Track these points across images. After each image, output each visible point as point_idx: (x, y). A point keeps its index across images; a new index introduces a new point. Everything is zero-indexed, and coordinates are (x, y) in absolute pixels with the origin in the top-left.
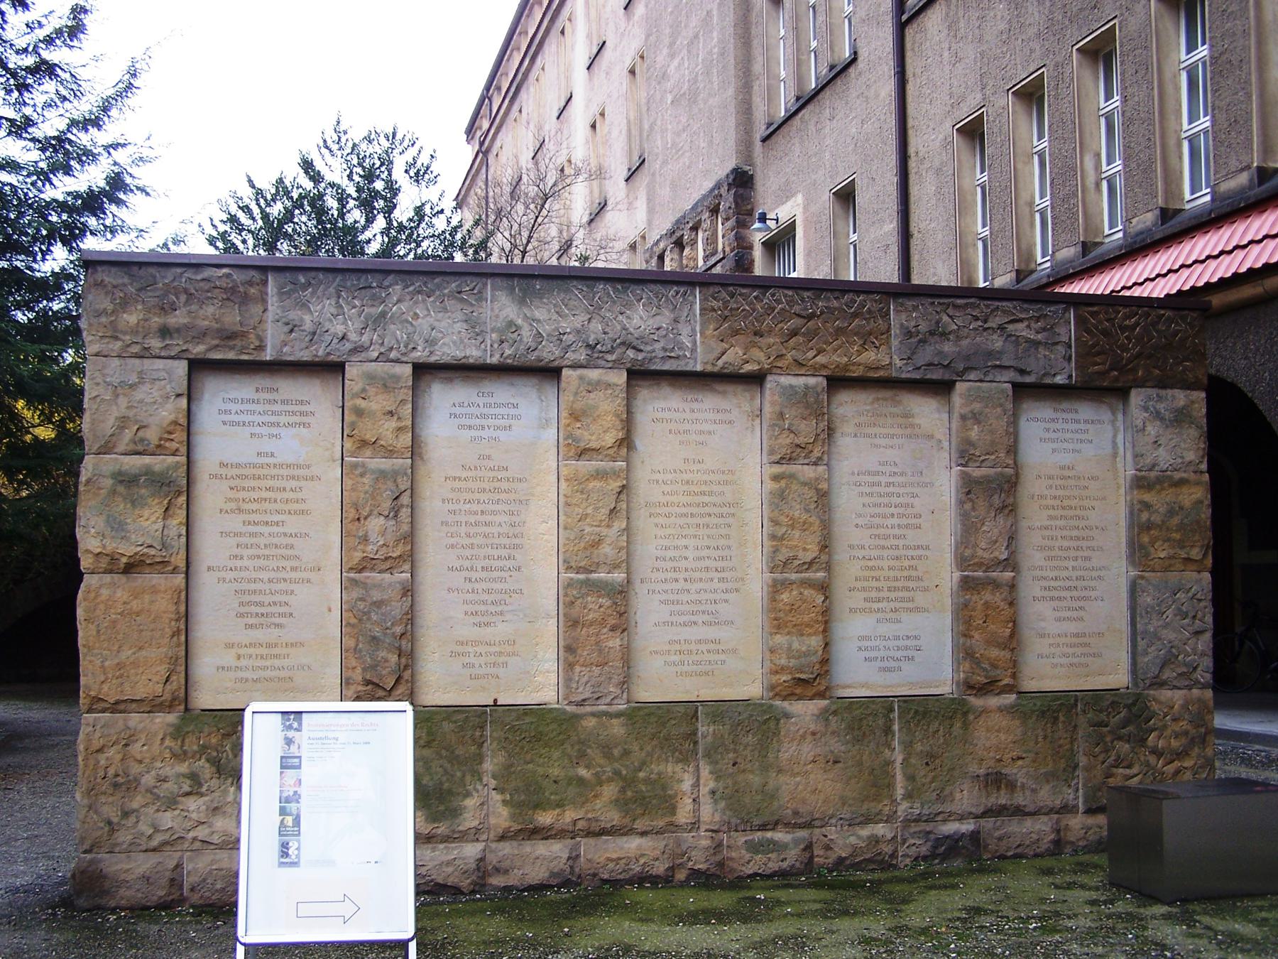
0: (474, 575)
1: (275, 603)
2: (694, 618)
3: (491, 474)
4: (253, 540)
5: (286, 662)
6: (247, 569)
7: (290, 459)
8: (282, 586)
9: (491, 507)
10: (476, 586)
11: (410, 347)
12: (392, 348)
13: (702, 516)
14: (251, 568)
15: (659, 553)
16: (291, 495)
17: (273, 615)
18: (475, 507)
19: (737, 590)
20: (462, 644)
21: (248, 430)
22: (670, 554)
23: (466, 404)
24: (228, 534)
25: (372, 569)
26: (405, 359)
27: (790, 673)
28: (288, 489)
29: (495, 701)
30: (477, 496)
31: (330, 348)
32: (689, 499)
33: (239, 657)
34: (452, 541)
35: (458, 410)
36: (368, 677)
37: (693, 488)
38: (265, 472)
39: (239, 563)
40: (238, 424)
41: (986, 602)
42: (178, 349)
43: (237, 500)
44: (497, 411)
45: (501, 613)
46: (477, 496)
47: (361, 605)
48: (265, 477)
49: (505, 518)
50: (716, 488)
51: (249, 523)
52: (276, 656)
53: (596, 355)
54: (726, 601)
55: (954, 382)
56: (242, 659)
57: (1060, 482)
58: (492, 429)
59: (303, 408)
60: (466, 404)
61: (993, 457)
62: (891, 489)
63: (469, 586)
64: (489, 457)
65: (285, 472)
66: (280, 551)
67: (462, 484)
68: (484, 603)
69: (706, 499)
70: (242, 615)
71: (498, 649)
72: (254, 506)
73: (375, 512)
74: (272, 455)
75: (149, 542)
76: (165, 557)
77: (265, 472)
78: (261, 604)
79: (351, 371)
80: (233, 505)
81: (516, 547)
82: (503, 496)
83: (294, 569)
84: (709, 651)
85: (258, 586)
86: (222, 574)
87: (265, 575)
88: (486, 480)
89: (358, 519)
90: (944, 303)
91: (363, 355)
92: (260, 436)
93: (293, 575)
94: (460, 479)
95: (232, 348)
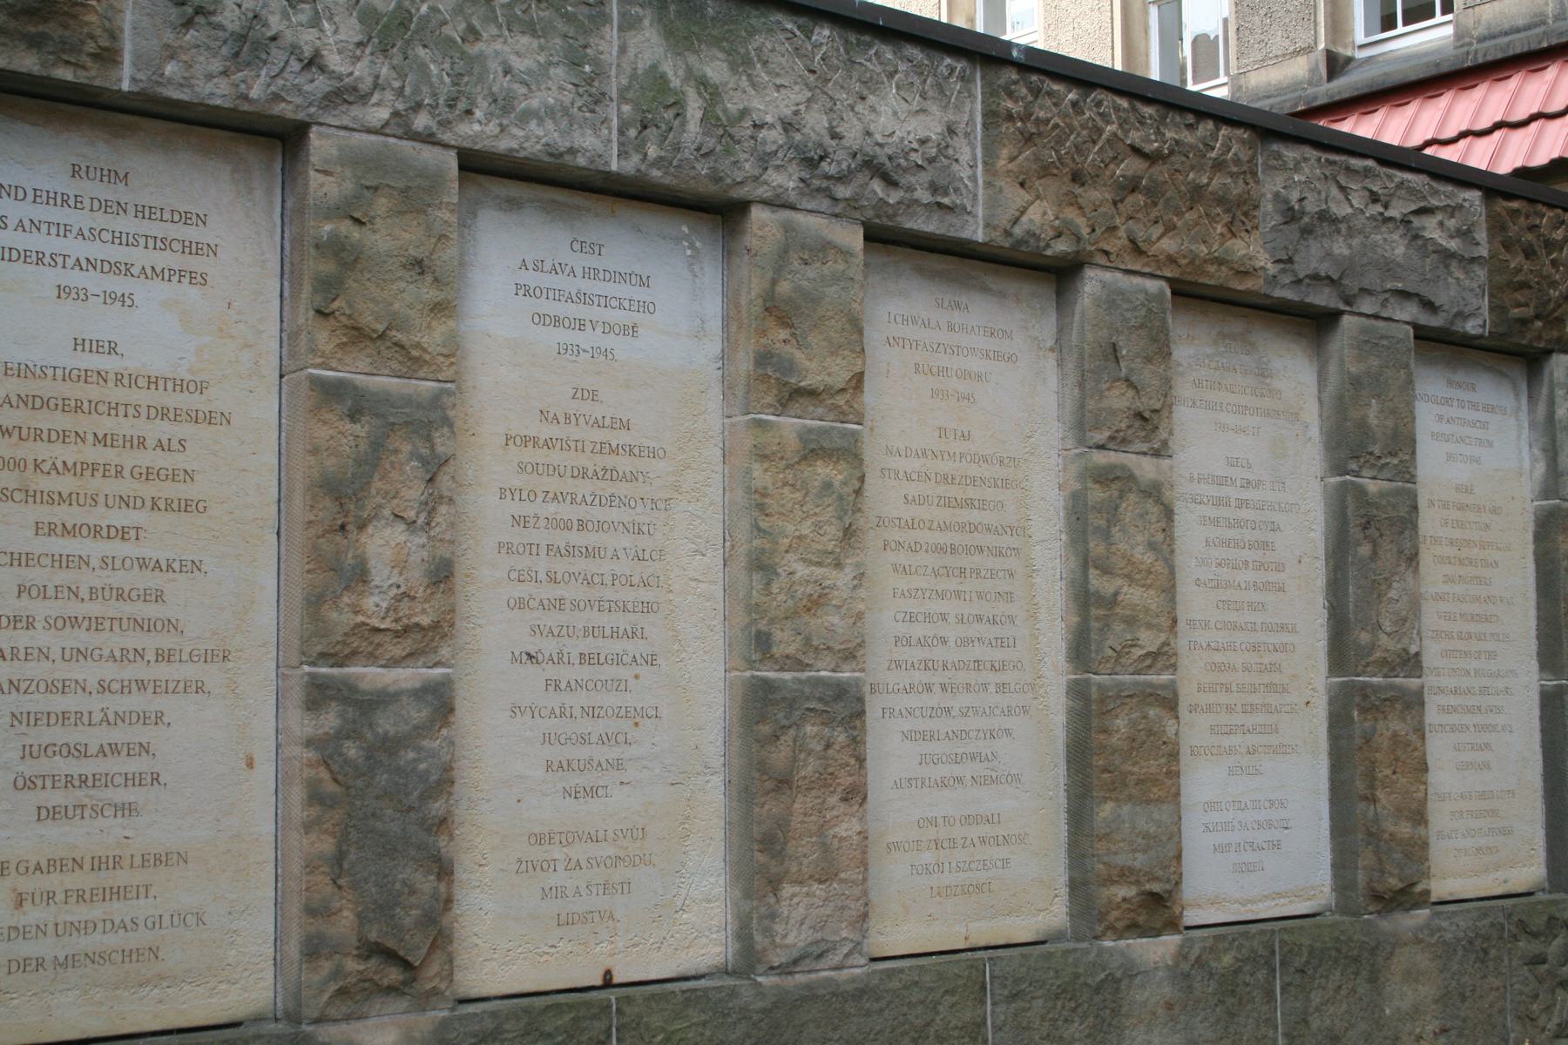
0: (566, 674)
1: (115, 749)
2: (957, 770)
3: (599, 435)
4: (63, 577)
5: (142, 908)
6: (44, 654)
7: (159, 365)
8: (135, 702)
9: (598, 513)
10: (569, 699)
12: (418, 107)
13: (968, 550)
14: (55, 653)
15: (902, 629)
16: (161, 460)
17: (108, 780)
18: (566, 511)
19: (1025, 710)
20: (540, 839)
21: (52, 276)
22: (918, 630)
23: (548, 267)
25: (372, 658)
26: (447, 137)
27: (1138, 882)
28: (150, 443)
29: (608, 973)
30: (569, 485)
31: (280, 82)
32: (944, 515)
34: (520, 591)
35: (532, 279)
36: (373, 936)
37: (954, 491)
38: (94, 392)
40: (24, 256)
41: (1395, 735)
44: (610, 289)
45: (618, 765)
46: (569, 485)
47: (352, 750)
48: (94, 407)
49: (625, 541)
50: (990, 494)
51: (52, 530)
52: (119, 893)
53: (816, 183)
54: (1008, 732)
55: (1341, 313)
56: (27, 906)
57: (1455, 514)
58: (599, 329)
59: (192, 233)
60: (548, 267)
61: (1396, 461)
62: (1245, 514)
63: (554, 700)
64: (594, 396)
65: (142, 397)
66: (128, 609)
67: (540, 456)
68: (584, 740)
69: (975, 516)
70: (29, 784)
71: (612, 851)
72: (66, 484)
73: (387, 512)
74: (113, 349)
77: (94, 392)
78: (81, 752)
79: (320, 144)
81: (648, 608)
82: (622, 489)
83: (163, 656)
84: (983, 841)
85: (70, 702)
87: (89, 673)
88: (589, 447)
89: (343, 527)
90: (1335, 163)
91: (356, 111)
92: (82, 295)
93: (163, 671)
94: (535, 441)
95: (35, 43)
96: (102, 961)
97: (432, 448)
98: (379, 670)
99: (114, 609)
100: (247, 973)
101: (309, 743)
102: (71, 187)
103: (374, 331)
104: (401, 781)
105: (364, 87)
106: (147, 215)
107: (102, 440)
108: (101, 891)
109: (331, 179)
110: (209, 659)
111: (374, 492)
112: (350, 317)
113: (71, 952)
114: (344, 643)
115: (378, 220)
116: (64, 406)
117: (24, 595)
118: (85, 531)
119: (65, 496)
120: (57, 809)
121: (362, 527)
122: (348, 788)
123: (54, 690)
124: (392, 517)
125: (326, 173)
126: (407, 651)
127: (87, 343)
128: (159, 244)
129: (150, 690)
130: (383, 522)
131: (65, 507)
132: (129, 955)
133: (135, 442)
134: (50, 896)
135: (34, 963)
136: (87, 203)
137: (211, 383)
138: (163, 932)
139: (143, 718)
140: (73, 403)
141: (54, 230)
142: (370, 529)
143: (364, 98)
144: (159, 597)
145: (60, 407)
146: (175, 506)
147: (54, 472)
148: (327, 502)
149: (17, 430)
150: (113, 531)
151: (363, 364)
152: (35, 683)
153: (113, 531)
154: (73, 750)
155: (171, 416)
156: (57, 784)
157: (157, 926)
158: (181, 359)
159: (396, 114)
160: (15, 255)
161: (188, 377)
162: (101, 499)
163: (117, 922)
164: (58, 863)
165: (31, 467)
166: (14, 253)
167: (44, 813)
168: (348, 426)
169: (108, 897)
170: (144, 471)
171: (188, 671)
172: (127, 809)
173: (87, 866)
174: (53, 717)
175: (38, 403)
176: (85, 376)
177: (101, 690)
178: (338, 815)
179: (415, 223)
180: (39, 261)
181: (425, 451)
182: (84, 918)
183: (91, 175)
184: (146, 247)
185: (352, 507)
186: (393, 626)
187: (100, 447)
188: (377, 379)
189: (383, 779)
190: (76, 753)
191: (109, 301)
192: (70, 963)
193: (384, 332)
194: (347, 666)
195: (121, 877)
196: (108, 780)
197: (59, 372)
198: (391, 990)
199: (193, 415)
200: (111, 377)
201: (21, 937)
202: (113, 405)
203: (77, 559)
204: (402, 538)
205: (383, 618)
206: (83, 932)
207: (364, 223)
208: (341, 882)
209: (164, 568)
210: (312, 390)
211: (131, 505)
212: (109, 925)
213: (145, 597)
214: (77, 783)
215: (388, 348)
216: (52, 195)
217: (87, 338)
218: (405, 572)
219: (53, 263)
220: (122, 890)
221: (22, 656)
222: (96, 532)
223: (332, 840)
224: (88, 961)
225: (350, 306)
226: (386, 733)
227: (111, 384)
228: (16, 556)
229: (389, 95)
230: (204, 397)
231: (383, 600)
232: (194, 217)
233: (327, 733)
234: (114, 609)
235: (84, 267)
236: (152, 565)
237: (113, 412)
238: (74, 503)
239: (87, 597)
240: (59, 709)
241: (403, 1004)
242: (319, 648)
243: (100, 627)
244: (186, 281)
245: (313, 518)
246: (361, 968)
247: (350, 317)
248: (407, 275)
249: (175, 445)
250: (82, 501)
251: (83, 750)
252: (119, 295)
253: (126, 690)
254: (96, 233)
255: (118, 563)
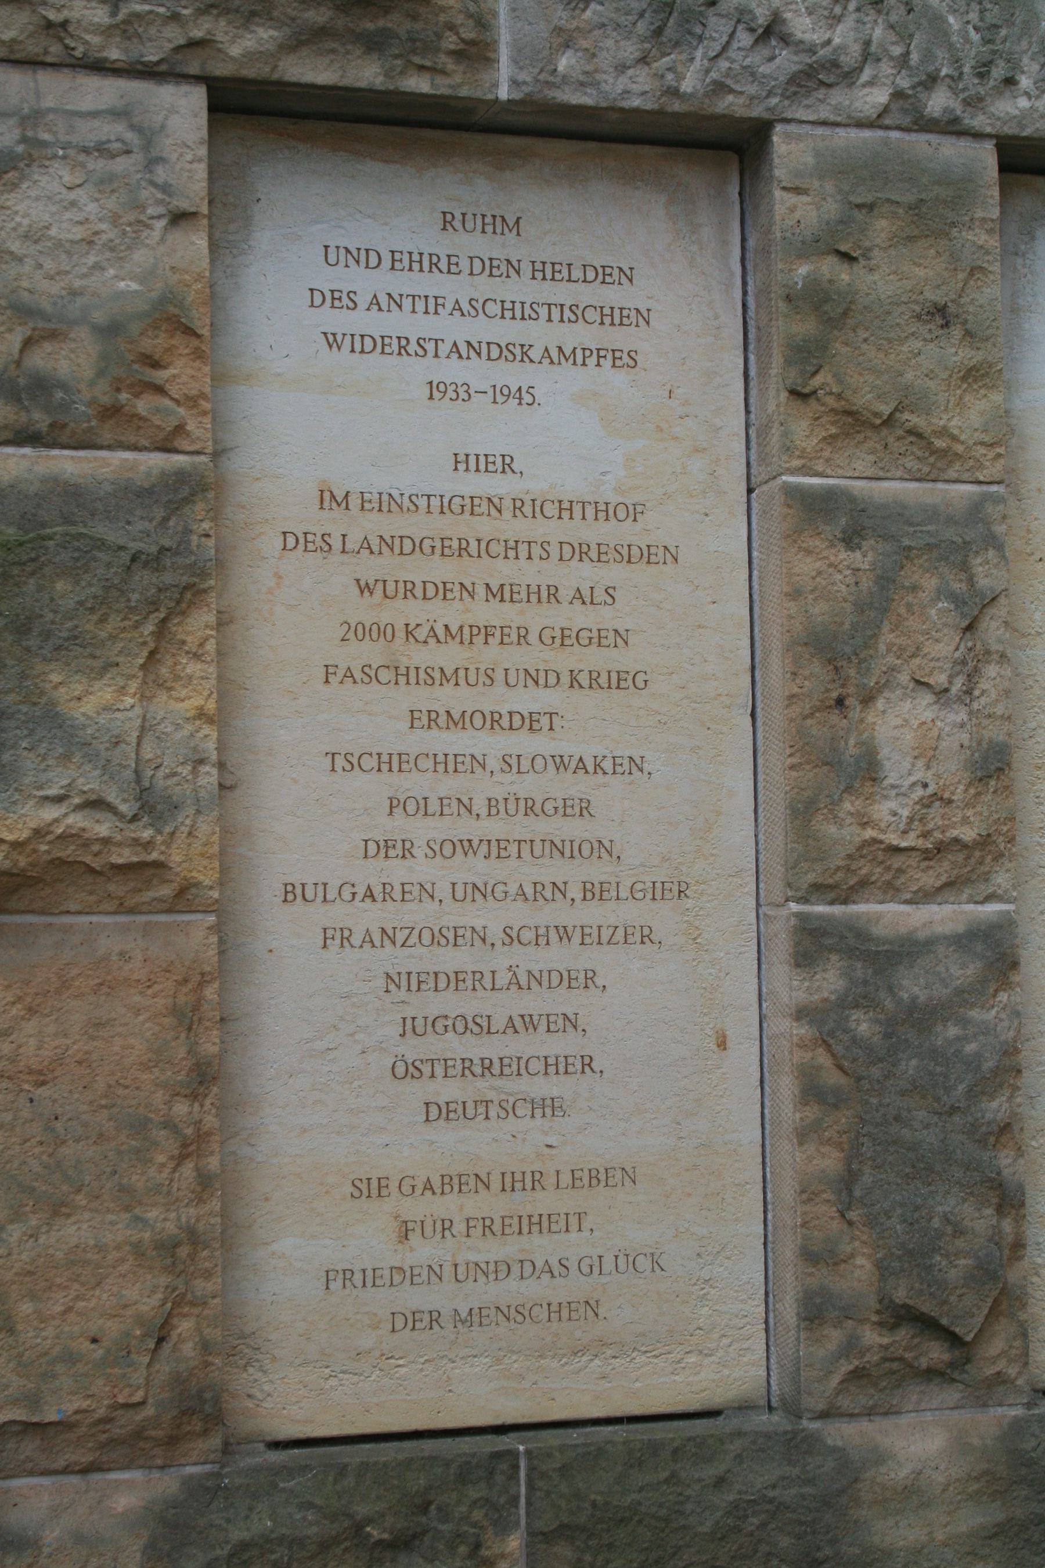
1: (529, 1023)
4: (450, 785)
11: (998, 72)
12: (931, 81)
14: (443, 890)
16: (580, 617)
17: (521, 1067)
24: (353, 763)
25: (891, 890)
26: (979, 122)
31: (724, 64)
33: (405, 1235)
36: (900, 1295)
38: (484, 526)
39: (397, 871)
40: (381, 345)
42: (174, 36)
43: (383, 633)
47: (863, 1025)
48: (485, 546)
51: (432, 719)
52: (541, 1223)
56: (415, 1238)
59: (612, 296)
70: (413, 1071)
73: (904, 678)
74: (507, 465)
75: (91, 782)
76: (148, 846)
77: (484, 526)
78: (481, 1026)
80: (371, 652)
83: (593, 892)
86: (337, 914)
89: (840, 702)
91: (838, 96)
92: (463, 393)
93: (592, 914)
96: (520, 1318)
97: (971, 581)
98: (903, 908)
99: (521, 827)
100: (725, 1341)
101: (801, 1014)
102: (440, 244)
103: (876, 414)
104: (939, 1069)
105: (848, 60)
106: (549, 276)
107: (497, 593)
108: (516, 1220)
109: (805, 199)
110: (658, 896)
111: (882, 648)
112: (839, 396)
113: (476, 1305)
114: (848, 869)
115: (876, 252)
116: (444, 548)
117: (398, 811)
118: (478, 721)
119: (449, 672)
120: (452, 1107)
121: (868, 700)
122: (859, 1079)
123: (443, 941)
124: (912, 685)
125: (797, 191)
126: (944, 879)
127: (472, 460)
128: (567, 313)
129: (576, 939)
130: (899, 692)
131: (449, 688)
132: (556, 1311)
133: (544, 594)
134: (446, 1227)
135: (426, 1318)
136: (465, 264)
137: (647, 505)
138: (604, 1279)
139: (567, 979)
140: (455, 544)
141: (420, 306)
142: (880, 704)
143: (849, 77)
144: (585, 809)
145: (438, 551)
146: (603, 680)
147: (432, 641)
148: (816, 667)
149: (380, 585)
150: (517, 718)
151: (863, 464)
152: (416, 932)
153: (517, 718)
154: (471, 1025)
155: (594, 555)
156: (451, 1072)
157: (596, 1270)
158: (603, 474)
159: (898, 95)
160: (368, 343)
161: (614, 499)
162: (499, 676)
163: (539, 1264)
164: (456, 1180)
165: (401, 634)
166: (368, 341)
167: (434, 1111)
168: (843, 555)
169: (525, 1229)
170: (558, 633)
171: (629, 913)
172: (550, 1107)
173: (496, 1185)
174: (442, 978)
175: (408, 546)
176: (471, 506)
177: (507, 940)
178: (844, 1118)
179: (932, 252)
180: (402, 350)
181: (959, 587)
182: (492, 1257)
183: (469, 225)
184: (550, 320)
185: (852, 672)
186: (920, 843)
187: (494, 603)
188: (885, 484)
189: (910, 1066)
190: (476, 1029)
191: (500, 399)
192: (476, 1319)
193: (891, 414)
194: (854, 902)
195: (544, 1202)
196: (521, 1067)
197: (435, 502)
198: (931, 1374)
199: (625, 552)
200: (508, 503)
201: (408, 1281)
202: (512, 544)
203: (468, 759)
204: (929, 715)
205: (905, 832)
206: (492, 1277)
207: (854, 259)
208: (853, 1215)
209: (591, 768)
210: (789, 506)
211: (542, 681)
212: (528, 1268)
213: (564, 809)
214: (478, 1070)
215: (899, 439)
216: (415, 257)
217: (472, 451)
218: (934, 764)
219: (421, 352)
220: (545, 1219)
221: (397, 895)
222: (493, 721)
223: (836, 1154)
224: (501, 1317)
225: (840, 382)
226: (914, 999)
227: (507, 514)
228: (385, 758)
229: (886, 68)
230: (638, 526)
231: (903, 806)
232: (616, 271)
233: (825, 1000)
234: (521, 827)
235: (464, 354)
236: (573, 765)
237: (511, 554)
238: (462, 682)
239: (484, 812)
240: (450, 969)
241: (952, 1395)
242: (811, 877)
243: (503, 853)
244: (607, 363)
245: (796, 690)
246: (885, 1341)
247: (839, 396)
248: (923, 329)
249: (600, 596)
250: (472, 679)
251: (485, 1024)
252: (514, 390)
253: (542, 941)
254: (479, 306)
255: (525, 764)
